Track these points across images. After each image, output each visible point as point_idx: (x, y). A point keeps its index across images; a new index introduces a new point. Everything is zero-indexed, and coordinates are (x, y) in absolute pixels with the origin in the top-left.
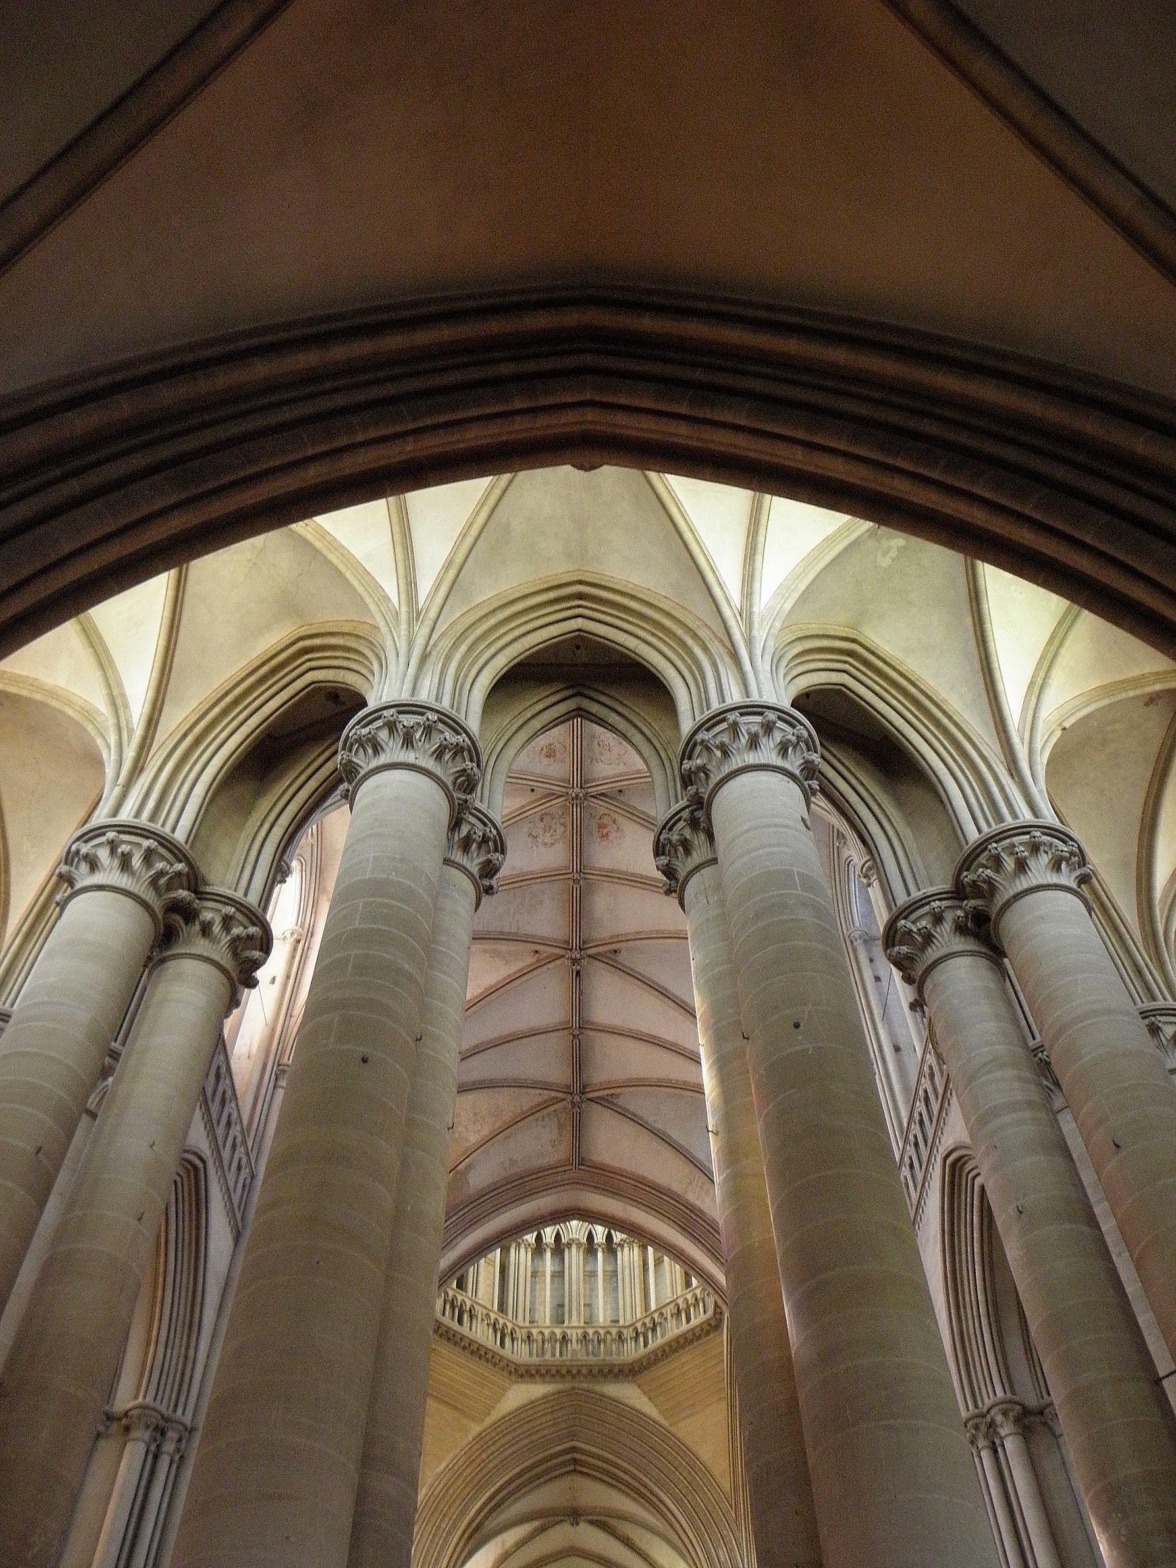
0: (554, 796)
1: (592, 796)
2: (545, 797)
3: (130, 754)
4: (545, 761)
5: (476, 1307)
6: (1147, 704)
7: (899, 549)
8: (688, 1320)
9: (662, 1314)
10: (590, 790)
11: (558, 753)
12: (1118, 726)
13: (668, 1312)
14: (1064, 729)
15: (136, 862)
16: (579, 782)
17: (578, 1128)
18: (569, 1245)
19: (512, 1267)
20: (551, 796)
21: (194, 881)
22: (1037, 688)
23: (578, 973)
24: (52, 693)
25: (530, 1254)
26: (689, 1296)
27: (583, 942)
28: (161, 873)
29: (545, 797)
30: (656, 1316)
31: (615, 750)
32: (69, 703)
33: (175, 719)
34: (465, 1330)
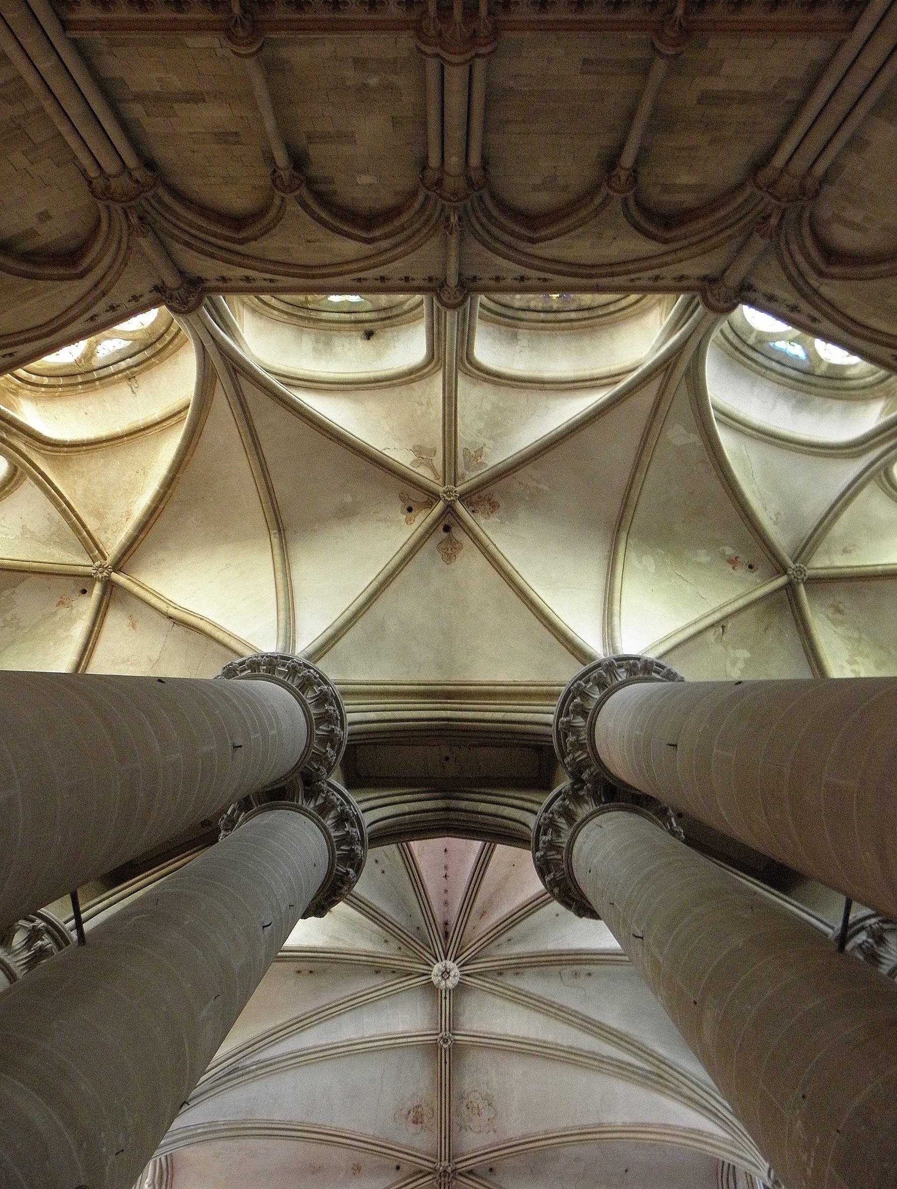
0: (421, 1175)
2: (411, 1176)
4: (412, 1128)
7: (746, 661)
10: (459, 1166)
11: (425, 1117)
16: (447, 1154)
20: (420, 1173)
27: (453, 1157)
29: (411, 1176)
31: (485, 1114)
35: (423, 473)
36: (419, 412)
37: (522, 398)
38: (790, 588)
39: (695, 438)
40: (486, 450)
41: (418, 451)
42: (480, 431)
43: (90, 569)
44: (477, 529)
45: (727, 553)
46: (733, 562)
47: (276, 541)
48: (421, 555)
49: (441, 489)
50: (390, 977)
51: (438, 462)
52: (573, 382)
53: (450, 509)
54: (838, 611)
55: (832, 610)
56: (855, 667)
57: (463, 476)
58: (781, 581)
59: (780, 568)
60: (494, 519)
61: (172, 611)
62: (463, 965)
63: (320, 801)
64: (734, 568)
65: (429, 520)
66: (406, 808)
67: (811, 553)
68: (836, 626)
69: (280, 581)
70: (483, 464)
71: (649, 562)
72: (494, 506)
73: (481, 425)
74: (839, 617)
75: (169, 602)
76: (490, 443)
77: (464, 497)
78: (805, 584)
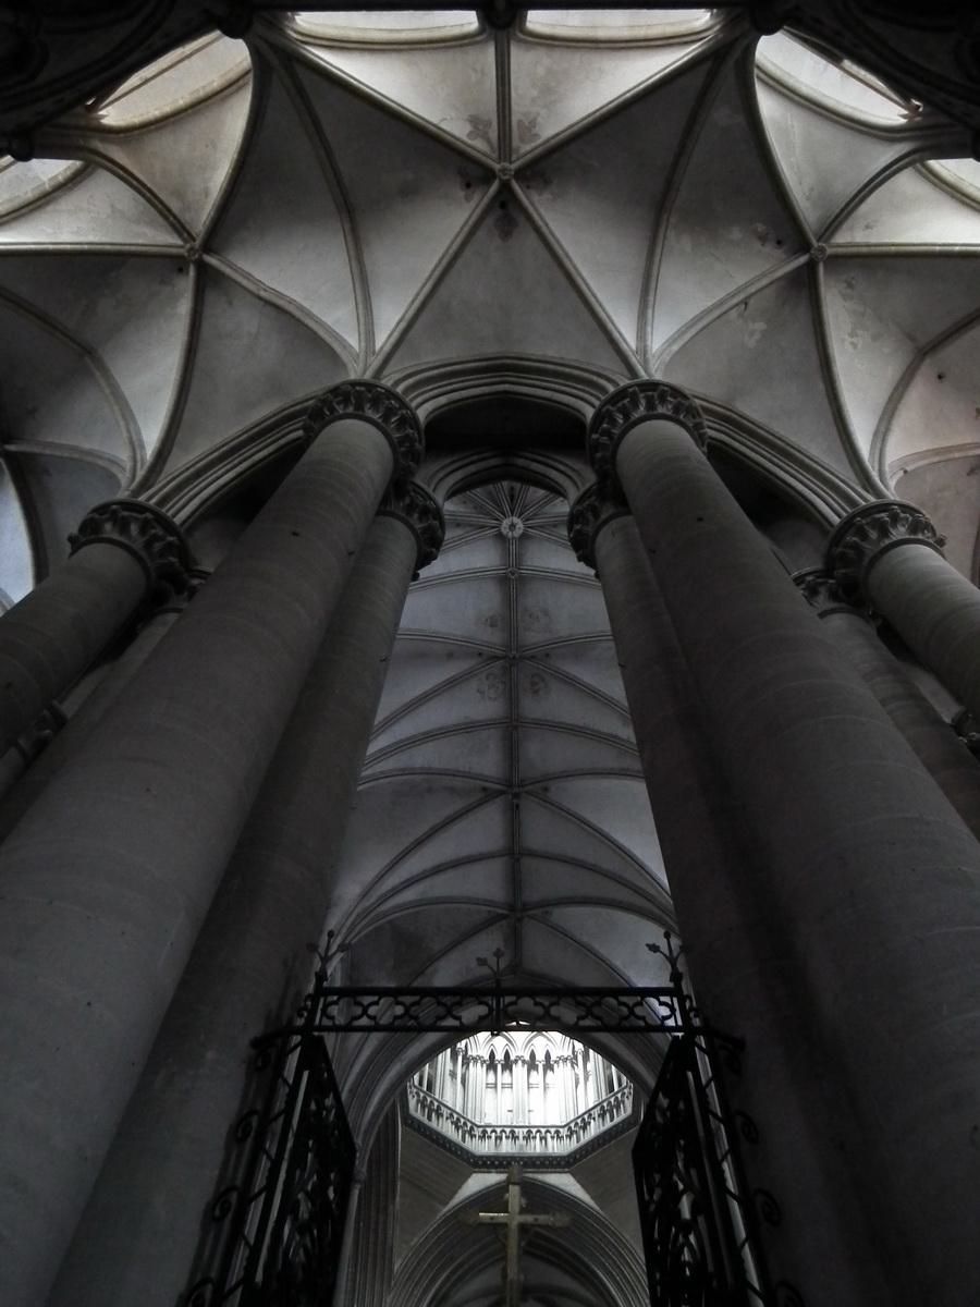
1: (528, 659)
3: (140, 474)
5: (442, 1108)
6: (968, 474)
8: (612, 1119)
9: (590, 1115)
12: (946, 494)
13: (596, 1112)
14: (905, 472)
15: (134, 529)
17: (515, 939)
18: (516, 1061)
19: (471, 1079)
20: (496, 658)
21: (183, 552)
22: (881, 435)
23: (517, 806)
24: (90, 453)
25: (485, 1068)
26: (612, 1100)
28: (156, 538)
30: (586, 1116)
32: (101, 458)
33: (180, 462)
34: (433, 1124)
35: (480, 146)
36: (473, 79)
37: (575, 59)
38: (811, 267)
39: (740, 119)
40: (539, 119)
41: (475, 121)
42: (534, 100)
43: (182, 251)
44: (531, 209)
45: (759, 230)
46: (763, 239)
47: (347, 226)
48: (481, 234)
49: (497, 166)
50: (468, 529)
51: (493, 134)
52: (627, 41)
53: (505, 187)
54: (850, 286)
55: (845, 285)
56: (855, 340)
57: (518, 149)
58: (803, 259)
59: (804, 246)
60: (547, 195)
61: (263, 294)
62: (527, 520)
63: (407, 500)
64: (763, 245)
65: (486, 200)
66: (473, 468)
67: (833, 233)
68: (845, 300)
69: (356, 271)
70: (536, 135)
71: (686, 242)
72: (547, 182)
73: (535, 93)
74: (849, 291)
75: (257, 282)
76: (543, 112)
77: (520, 174)
78: (824, 262)
